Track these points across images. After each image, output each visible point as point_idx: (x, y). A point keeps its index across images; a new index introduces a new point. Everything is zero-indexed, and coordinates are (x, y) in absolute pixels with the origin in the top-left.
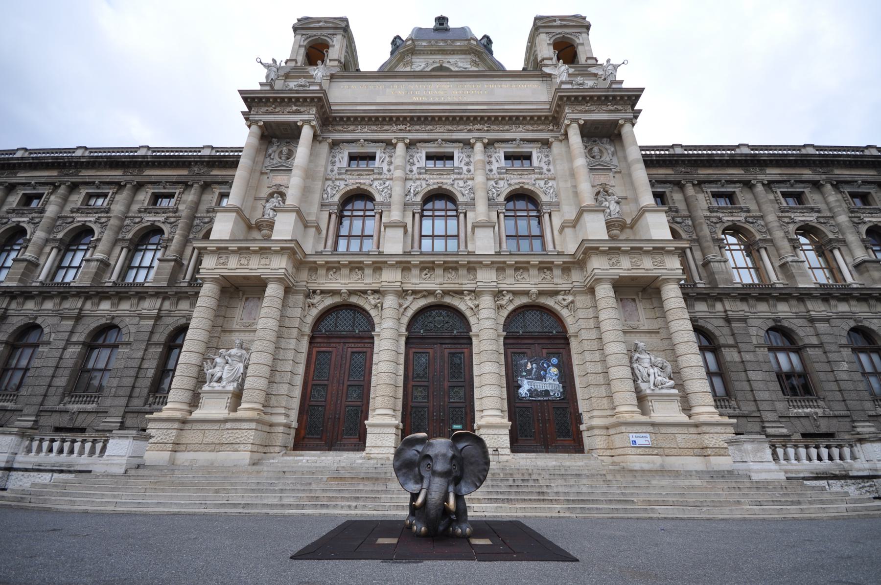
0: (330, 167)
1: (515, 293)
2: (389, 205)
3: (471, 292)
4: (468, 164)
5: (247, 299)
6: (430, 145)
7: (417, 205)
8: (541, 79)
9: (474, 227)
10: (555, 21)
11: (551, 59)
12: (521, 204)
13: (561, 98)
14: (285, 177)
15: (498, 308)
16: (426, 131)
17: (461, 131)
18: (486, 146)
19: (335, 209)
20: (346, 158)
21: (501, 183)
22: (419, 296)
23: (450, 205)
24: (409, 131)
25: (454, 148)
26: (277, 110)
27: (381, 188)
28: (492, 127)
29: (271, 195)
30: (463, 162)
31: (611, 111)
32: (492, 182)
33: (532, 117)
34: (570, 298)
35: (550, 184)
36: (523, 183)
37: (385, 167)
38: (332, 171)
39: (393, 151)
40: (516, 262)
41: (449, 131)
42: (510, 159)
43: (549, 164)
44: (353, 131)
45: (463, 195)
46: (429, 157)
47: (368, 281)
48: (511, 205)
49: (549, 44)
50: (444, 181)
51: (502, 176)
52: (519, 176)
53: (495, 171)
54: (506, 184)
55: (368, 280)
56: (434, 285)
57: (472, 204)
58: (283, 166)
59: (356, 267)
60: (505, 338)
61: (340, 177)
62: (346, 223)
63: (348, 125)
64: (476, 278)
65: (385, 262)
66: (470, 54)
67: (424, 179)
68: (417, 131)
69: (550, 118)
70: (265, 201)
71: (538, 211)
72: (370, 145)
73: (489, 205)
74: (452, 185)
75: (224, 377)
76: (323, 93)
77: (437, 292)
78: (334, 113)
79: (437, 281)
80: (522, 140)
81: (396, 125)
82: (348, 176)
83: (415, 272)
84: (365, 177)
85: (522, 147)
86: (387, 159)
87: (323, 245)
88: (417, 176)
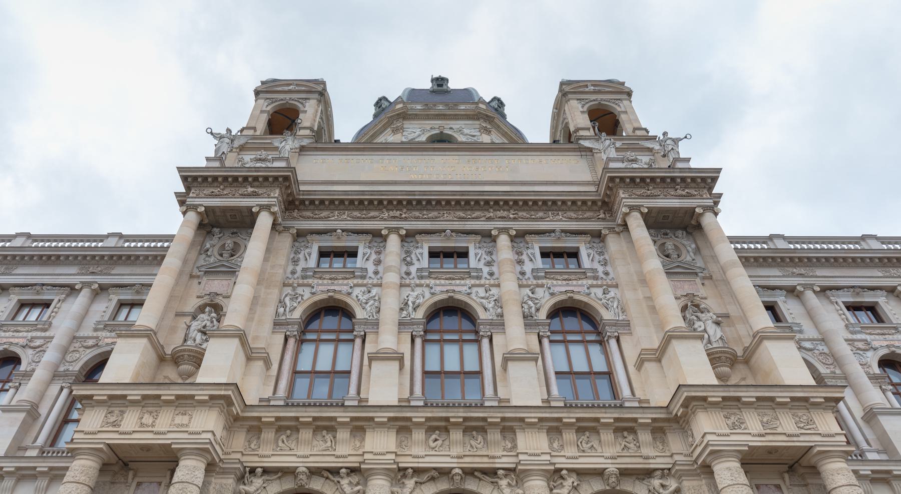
2: (376, 324)
5: (139, 484)
6: (434, 237)
7: (418, 324)
8: (579, 154)
9: (506, 360)
10: (587, 86)
11: (588, 129)
12: (572, 323)
13: (612, 179)
14: (225, 283)
16: (429, 219)
17: (477, 219)
18: (513, 239)
19: (294, 330)
22: (425, 477)
23: (466, 325)
24: (406, 219)
25: (469, 241)
26: (225, 193)
27: (363, 298)
28: (520, 214)
29: (201, 309)
30: (483, 261)
32: (527, 291)
33: (574, 202)
36: (573, 292)
37: (371, 268)
38: (293, 272)
39: (382, 245)
40: (579, 420)
41: (461, 219)
42: (549, 257)
44: (326, 218)
45: (486, 309)
46: (433, 254)
48: (556, 323)
49: (582, 112)
50: (457, 289)
51: (540, 282)
52: (564, 282)
53: (529, 274)
54: (547, 293)
55: (342, 450)
56: (448, 459)
57: (500, 324)
58: (223, 266)
61: (305, 281)
63: (321, 210)
64: (515, 447)
65: (371, 419)
66: (478, 119)
67: (428, 286)
68: (417, 218)
69: (600, 203)
70: (190, 318)
71: (599, 333)
72: (349, 238)
73: (526, 325)
74: (469, 294)
76: (292, 172)
77: (454, 472)
78: (303, 195)
79: (456, 451)
80: (563, 231)
81: (388, 210)
82: (316, 281)
83: (419, 435)
84: (341, 282)
85: (565, 241)
86: (374, 257)
87: (272, 388)
88: (418, 282)
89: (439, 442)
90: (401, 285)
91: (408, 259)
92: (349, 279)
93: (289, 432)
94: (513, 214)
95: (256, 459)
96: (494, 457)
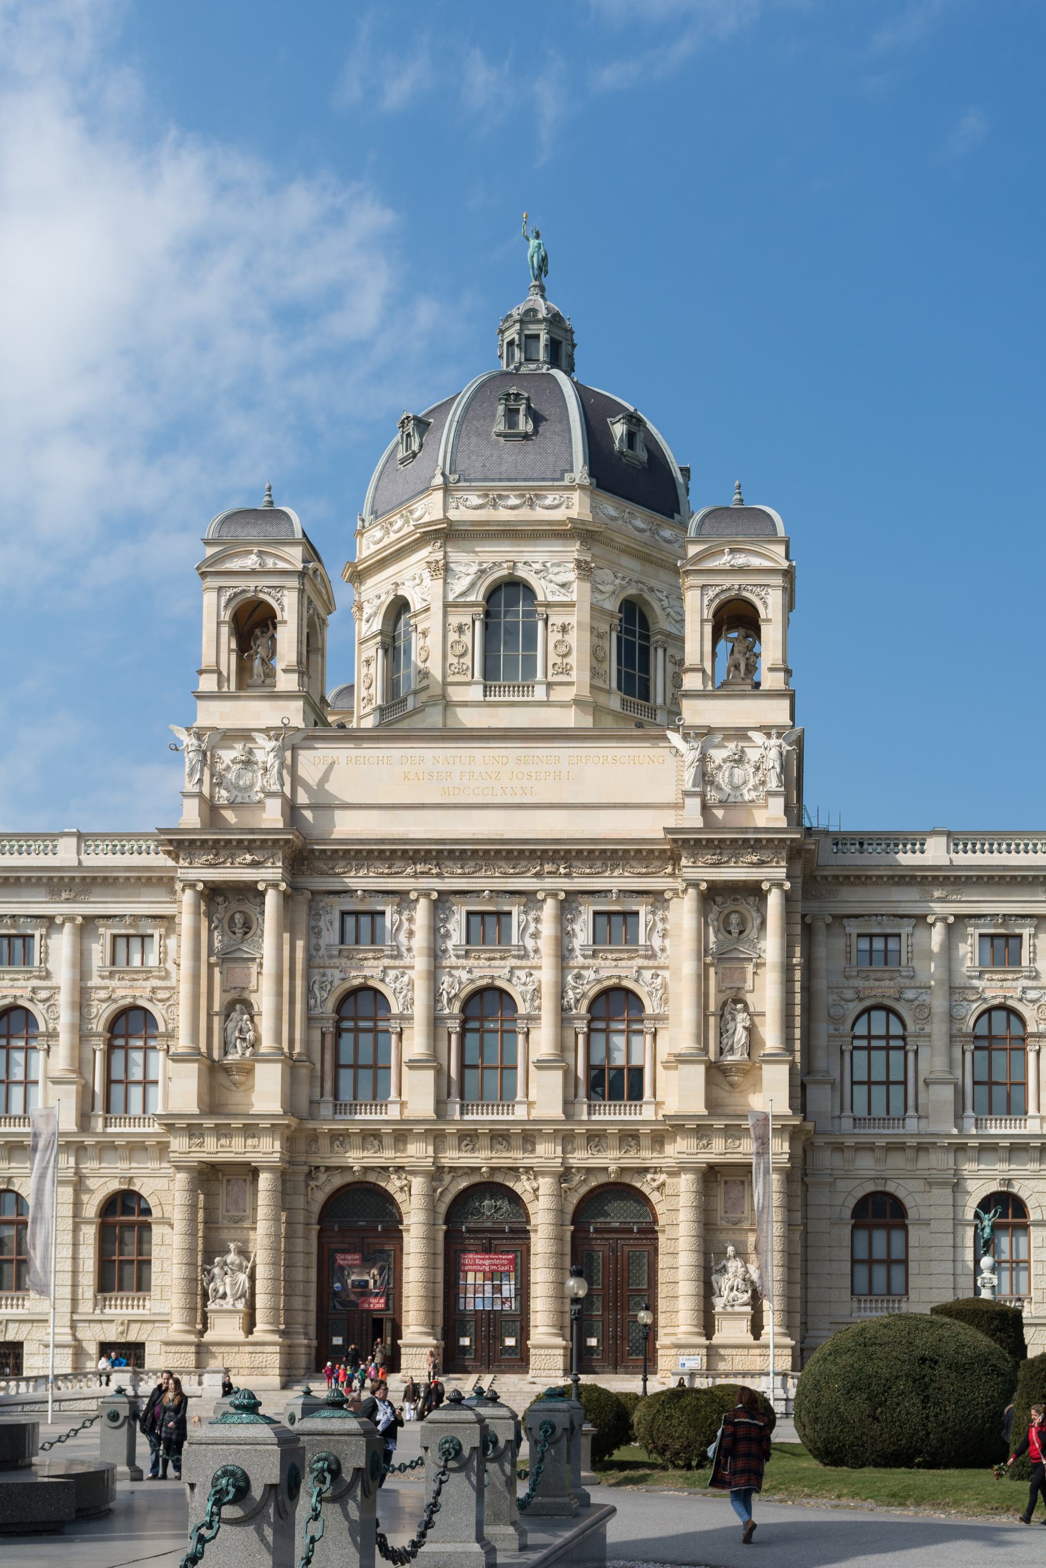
0: (314, 941)
1: (589, 1170)
2: (410, 1018)
3: (528, 1169)
4: (536, 936)
5: (228, 1181)
15: (566, 1192)
19: (330, 1027)
20: (337, 924)
21: (584, 972)
25: (512, 904)
31: (753, 865)
34: (662, 1178)
35: (659, 980)
41: (506, 875)
43: (664, 936)
47: (387, 1156)
52: (614, 963)
56: (479, 1161)
59: (371, 1136)
60: (573, 1233)
62: (347, 1039)
67: (464, 968)
69: (669, 854)
73: (563, 1020)
75: (228, 1291)
77: (484, 1170)
82: (344, 961)
89: (470, 1147)
90: (436, 967)
91: (442, 931)
92: (378, 958)
93: (341, 1138)
94: (565, 868)
95: (319, 1160)
96: (515, 1159)
